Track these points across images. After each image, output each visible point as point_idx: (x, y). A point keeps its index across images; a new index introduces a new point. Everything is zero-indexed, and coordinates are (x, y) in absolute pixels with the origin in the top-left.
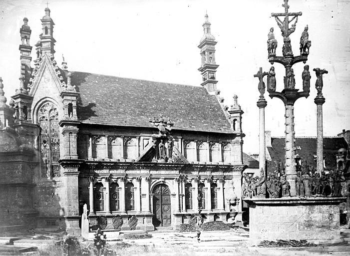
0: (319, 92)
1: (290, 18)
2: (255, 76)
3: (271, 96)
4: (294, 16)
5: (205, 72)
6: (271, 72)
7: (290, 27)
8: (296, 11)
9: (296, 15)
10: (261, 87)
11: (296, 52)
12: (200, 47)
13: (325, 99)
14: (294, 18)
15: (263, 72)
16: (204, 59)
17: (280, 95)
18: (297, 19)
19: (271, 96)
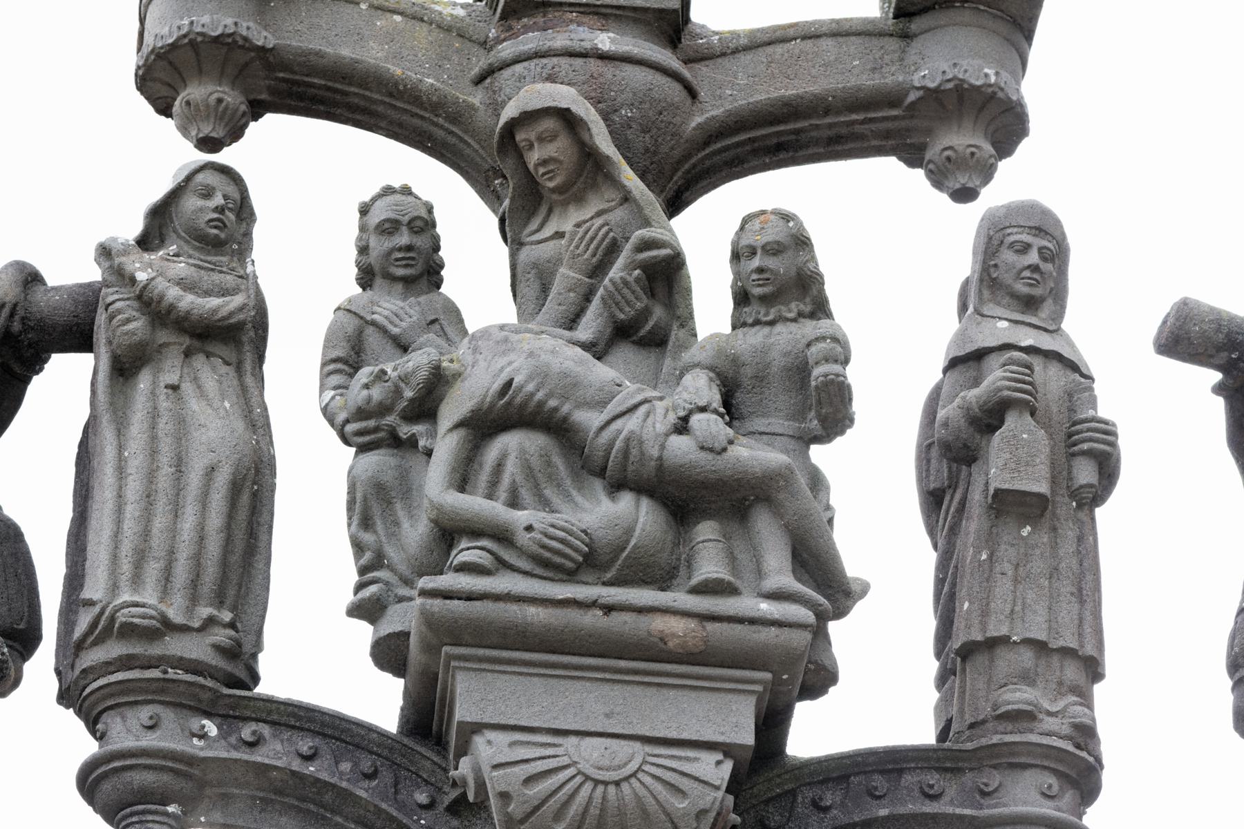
6: (167, 272)
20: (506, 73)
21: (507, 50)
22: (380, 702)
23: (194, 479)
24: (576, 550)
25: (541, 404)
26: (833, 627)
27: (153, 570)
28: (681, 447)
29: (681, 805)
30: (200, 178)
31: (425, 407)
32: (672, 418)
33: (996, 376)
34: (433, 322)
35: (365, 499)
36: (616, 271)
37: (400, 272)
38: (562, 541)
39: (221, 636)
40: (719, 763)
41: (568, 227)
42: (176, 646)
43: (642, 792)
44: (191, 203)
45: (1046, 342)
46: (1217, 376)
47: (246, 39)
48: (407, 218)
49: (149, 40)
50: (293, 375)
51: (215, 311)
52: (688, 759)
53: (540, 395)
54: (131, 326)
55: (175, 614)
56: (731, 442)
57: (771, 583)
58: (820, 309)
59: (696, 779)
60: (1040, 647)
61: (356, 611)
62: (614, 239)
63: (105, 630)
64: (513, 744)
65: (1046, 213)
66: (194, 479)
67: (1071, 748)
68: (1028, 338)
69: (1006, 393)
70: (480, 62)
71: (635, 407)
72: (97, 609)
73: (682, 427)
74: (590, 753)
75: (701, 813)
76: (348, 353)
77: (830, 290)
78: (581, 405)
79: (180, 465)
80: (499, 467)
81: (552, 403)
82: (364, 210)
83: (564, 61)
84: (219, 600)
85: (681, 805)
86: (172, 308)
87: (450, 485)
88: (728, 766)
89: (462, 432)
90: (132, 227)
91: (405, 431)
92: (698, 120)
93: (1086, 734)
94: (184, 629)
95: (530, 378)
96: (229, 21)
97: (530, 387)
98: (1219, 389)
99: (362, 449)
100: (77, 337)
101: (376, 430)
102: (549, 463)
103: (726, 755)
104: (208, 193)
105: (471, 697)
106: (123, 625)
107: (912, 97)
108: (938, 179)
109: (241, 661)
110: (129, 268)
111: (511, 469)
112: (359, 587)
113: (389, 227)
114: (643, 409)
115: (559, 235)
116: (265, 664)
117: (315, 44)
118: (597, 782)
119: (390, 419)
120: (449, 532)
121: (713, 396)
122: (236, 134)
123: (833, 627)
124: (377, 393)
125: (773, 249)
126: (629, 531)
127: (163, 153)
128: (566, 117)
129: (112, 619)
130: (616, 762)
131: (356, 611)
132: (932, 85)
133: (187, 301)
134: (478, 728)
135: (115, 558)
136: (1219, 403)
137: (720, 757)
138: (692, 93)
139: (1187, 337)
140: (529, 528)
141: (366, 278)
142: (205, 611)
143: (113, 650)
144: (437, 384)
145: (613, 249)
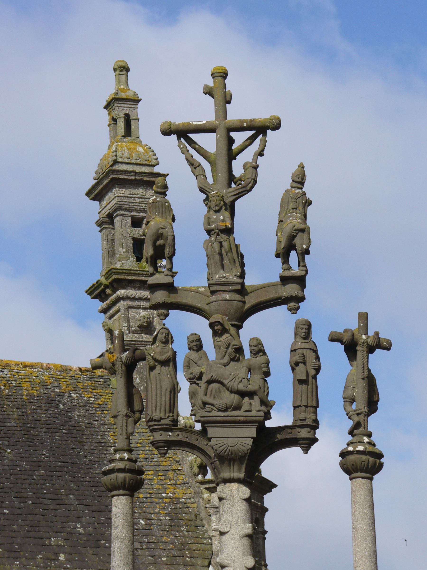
0: (358, 429)
4: (251, 133)
5: (114, 303)
7: (238, 169)
8: (261, 114)
12: (97, 194)
13: (380, 456)
14: (252, 139)
16: (110, 252)
18: (264, 144)
25: (218, 380)
27: (158, 408)
29: (244, 449)
30: (161, 331)
31: (200, 378)
32: (239, 380)
37: (195, 349)
39: (170, 419)
41: (222, 340)
42: (163, 422)
43: (238, 447)
53: (217, 378)
57: (257, 409)
75: (248, 450)
79: (161, 387)
81: (219, 379)
83: (221, 302)
84: (170, 412)
86: (157, 360)
91: (197, 382)
92: (246, 307)
95: (215, 375)
104: (162, 334)
107: (283, 298)
110: (150, 353)
112: (192, 411)
114: (234, 379)
115: (221, 341)
117: (179, 301)
119: (195, 380)
120: (205, 404)
128: (219, 322)
132: (286, 296)
134: (211, 438)
138: (244, 302)
139: (334, 338)
142: (167, 415)
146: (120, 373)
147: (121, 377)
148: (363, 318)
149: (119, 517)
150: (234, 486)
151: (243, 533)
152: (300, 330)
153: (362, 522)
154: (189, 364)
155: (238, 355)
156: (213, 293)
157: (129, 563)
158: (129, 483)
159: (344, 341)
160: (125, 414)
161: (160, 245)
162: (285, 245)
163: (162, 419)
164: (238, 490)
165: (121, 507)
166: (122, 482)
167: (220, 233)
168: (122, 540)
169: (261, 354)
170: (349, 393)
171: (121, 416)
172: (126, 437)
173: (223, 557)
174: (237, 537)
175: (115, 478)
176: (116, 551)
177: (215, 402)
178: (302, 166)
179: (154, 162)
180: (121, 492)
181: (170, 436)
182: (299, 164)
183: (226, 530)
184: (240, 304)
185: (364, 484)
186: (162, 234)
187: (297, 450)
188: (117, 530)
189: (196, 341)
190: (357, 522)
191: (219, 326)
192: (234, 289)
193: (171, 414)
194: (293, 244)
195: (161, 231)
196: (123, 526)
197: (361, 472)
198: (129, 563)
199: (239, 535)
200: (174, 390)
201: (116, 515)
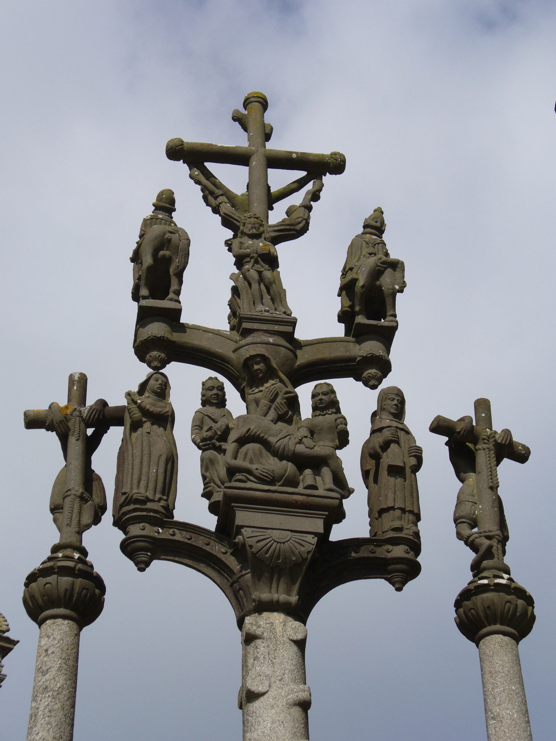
1: (279, 179)
2: (33, 422)
3: (139, 552)
6: (147, 401)
9: (319, 168)
10: (77, 500)
11: (316, 312)
14: (301, 183)
15: (90, 401)
17: (200, 542)
19: (139, 552)
20: (242, 349)
21: (243, 342)
22: (210, 522)
23: (154, 459)
24: (271, 475)
25: (259, 435)
26: (344, 501)
28: (300, 448)
29: (303, 549)
33: (387, 434)
34: (224, 415)
35: (207, 463)
36: (278, 400)
38: (266, 473)
39: (163, 503)
40: (313, 538)
42: (149, 505)
43: (291, 545)
44: (152, 382)
45: (400, 426)
46: (446, 439)
47: (167, 338)
48: (216, 386)
49: (138, 341)
50: (183, 432)
51: (160, 412)
52: (304, 536)
53: (258, 433)
54: (136, 415)
55: (151, 497)
56: (315, 446)
57: (327, 487)
58: (338, 411)
59: (307, 542)
60: (403, 510)
61: (203, 495)
62: (277, 392)
63: (129, 501)
64: (252, 532)
65: (399, 390)
66: (154, 459)
67: (413, 539)
68: (394, 424)
69: (391, 438)
70: (234, 346)
71: (287, 436)
72: (127, 495)
73: (300, 442)
74: (276, 534)
75: (309, 552)
76: (198, 424)
77: (341, 406)
78: (270, 436)
79: (150, 454)
80: (246, 454)
81: (262, 435)
82: (203, 384)
85: (303, 549)
87: (233, 458)
88: (316, 539)
89: (235, 444)
90: (135, 389)
92: (298, 363)
93: (417, 534)
94: (153, 501)
96: (163, 333)
97: (255, 430)
98: (447, 444)
99: (204, 451)
100: (119, 422)
101: (209, 444)
102: (261, 452)
103: (315, 536)
105: (242, 517)
106: (135, 499)
107: (359, 359)
108: (366, 384)
109: (169, 511)
110: (135, 399)
111: (250, 454)
113: (212, 388)
114: (288, 437)
115: (261, 391)
116: (175, 512)
118: (278, 542)
119: (214, 441)
120: (232, 471)
121: (308, 434)
122: (163, 366)
123: (344, 501)
124: (209, 434)
125: (325, 394)
126: (286, 471)
127: (143, 371)
129: (132, 497)
130: (283, 537)
131: (203, 495)
132: (365, 355)
133: (152, 409)
135: (132, 480)
136: (447, 448)
137: (313, 536)
138: (296, 356)
140: (257, 469)
141: (204, 403)
143: (132, 507)
144: (227, 431)
145: (277, 395)
146: (76, 432)
147: (78, 440)
148: (483, 406)
149: (53, 653)
150: (277, 618)
151: (292, 697)
152: (389, 402)
153: (510, 706)
154: (202, 423)
155: (290, 413)
156: (245, 333)
157: (64, 737)
158: (80, 594)
159: (458, 430)
160: (78, 493)
161: (164, 256)
162: (366, 282)
163: (148, 500)
164: (284, 625)
165: (59, 637)
166: (66, 590)
167: (259, 259)
168: (55, 694)
169: (334, 410)
170: (466, 509)
171: (72, 496)
172: (77, 529)
173: (255, 736)
174: (282, 703)
175: (54, 583)
176: (40, 713)
177: (253, 467)
178: (379, 212)
179: (4, 628)
180: (62, 611)
181: (162, 533)
182: (376, 208)
183: (261, 689)
184: (291, 354)
185: (507, 644)
186: (169, 241)
187: (378, 586)
188: (47, 676)
189: (217, 388)
190: (499, 705)
191: (262, 364)
192: (281, 330)
193: (165, 498)
194: (371, 298)
195: (168, 235)
196: (60, 669)
197: (501, 624)
198: (64, 737)
199: (287, 700)
200: (171, 461)
201: (46, 651)
